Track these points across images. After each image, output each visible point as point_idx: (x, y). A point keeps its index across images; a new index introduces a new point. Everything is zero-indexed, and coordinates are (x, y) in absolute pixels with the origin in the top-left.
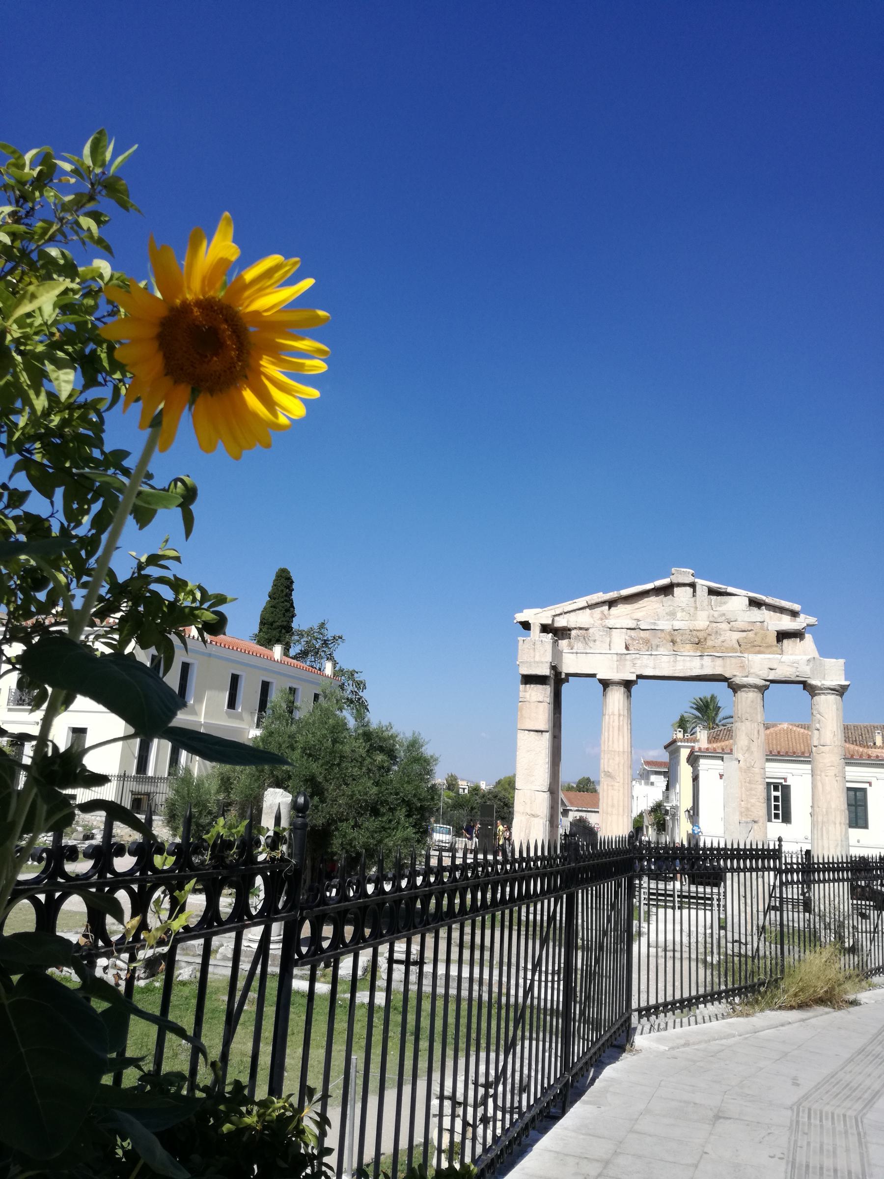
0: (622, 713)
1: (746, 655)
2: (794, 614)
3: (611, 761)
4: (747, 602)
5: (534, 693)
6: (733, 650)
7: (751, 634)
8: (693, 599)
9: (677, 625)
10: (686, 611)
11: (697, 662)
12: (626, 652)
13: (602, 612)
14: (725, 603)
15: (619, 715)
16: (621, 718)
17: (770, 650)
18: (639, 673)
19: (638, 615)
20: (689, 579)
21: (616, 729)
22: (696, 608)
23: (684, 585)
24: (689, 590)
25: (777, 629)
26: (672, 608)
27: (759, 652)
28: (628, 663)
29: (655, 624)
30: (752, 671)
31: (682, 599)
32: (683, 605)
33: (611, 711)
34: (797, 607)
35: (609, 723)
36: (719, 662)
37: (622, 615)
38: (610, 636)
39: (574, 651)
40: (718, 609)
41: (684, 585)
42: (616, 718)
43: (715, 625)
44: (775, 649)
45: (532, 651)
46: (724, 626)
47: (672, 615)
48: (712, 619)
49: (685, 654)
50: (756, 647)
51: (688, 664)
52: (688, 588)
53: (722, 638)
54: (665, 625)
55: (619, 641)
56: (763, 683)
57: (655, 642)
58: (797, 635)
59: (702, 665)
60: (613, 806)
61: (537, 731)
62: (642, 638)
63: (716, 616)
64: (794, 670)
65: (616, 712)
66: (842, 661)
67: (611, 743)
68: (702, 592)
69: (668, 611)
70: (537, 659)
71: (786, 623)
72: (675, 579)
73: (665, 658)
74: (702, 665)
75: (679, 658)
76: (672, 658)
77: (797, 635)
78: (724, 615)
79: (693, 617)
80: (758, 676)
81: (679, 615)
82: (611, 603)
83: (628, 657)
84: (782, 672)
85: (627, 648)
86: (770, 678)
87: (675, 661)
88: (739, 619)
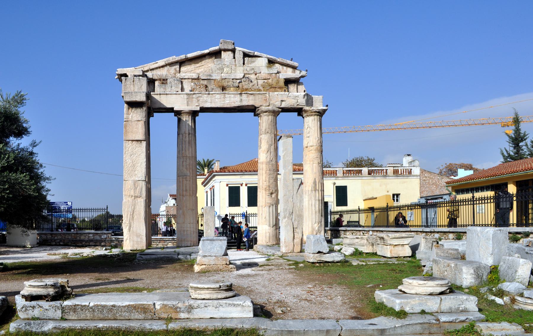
0: (190, 132)
1: (268, 93)
2: (294, 68)
3: (184, 163)
4: (267, 61)
5: (134, 115)
6: (260, 90)
9: (224, 75)
10: (230, 67)
11: (238, 98)
13: (175, 69)
16: (190, 135)
18: (201, 106)
19: (198, 71)
20: (231, 47)
21: (187, 142)
22: (236, 65)
24: (230, 54)
25: (285, 78)
26: (220, 65)
28: (194, 99)
33: (183, 131)
34: (296, 64)
36: (251, 97)
37: (188, 71)
40: (250, 65)
45: (132, 86)
48: (246, 72)
49: (230, 93)
50: (272, 88)
51: (232, 99)
52: (230, 52)
54: (216, 76)
56: (278, 109)
58: (296, 81)
59: (241, 100)
61: (137, 141)
62: (202, 85)
63: (248, 70)
65: (187, 132)
66: (321, 97)
67: (184, 151)
68: (239, 55)
69: (218, 67)
70: (136, 90)
71: (289, 73)
72: (222, 47)
75: (227, 96)
76: (222, 96)
77: (296, 81)
78: (253, 69)
81: (225, 70)
82: (181, 63)
83: (194, 96)
84: (289, 103)
86: (282, 106)
87: (225, 98)
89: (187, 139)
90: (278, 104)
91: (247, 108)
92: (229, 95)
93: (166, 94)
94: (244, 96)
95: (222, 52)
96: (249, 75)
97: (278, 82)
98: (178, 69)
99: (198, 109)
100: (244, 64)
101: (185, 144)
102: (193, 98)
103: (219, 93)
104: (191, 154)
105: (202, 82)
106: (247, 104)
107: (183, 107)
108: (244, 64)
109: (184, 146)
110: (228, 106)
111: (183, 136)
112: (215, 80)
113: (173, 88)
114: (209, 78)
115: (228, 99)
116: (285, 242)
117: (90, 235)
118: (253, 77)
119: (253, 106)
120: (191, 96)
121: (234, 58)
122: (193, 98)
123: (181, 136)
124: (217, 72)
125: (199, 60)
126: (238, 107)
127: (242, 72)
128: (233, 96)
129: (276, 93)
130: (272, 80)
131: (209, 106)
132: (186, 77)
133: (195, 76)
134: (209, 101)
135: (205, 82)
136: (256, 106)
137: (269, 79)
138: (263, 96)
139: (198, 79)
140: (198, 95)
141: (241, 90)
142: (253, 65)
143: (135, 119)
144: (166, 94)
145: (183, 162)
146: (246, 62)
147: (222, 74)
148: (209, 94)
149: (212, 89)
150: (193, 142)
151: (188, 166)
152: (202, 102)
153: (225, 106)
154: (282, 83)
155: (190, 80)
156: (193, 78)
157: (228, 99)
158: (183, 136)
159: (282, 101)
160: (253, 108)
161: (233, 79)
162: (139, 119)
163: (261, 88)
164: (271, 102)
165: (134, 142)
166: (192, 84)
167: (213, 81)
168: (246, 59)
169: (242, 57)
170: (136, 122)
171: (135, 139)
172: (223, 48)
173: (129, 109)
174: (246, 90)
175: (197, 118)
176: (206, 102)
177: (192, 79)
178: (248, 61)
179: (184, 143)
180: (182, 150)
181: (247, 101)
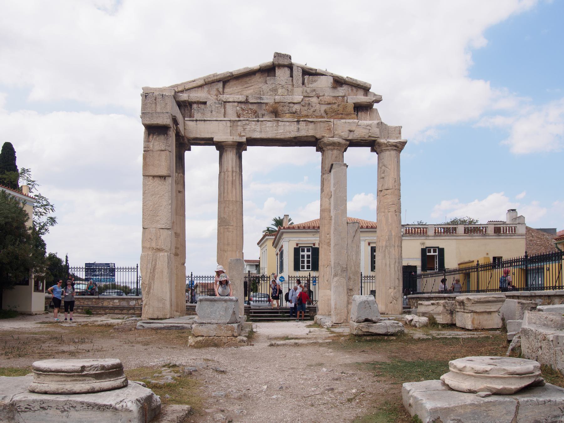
0: (234, 169)
1: (332, 120)
3: (226, 209)
5: (156, 143)
6: (322, 117)
7: (335, 106)
8: (291, 78)
9: (278, 98)
11: (294, 127)
12: (237, 119)
13: (218, 90)
14: (315, 81)
15: (233, 172)
16: (234, 174)
17: (350, 117)
18: (248, 136)
22: (293, 85)
23: (284, 66)
24: (287, 71)
25: (354, 101)
26: (274, 86)
27: (342, 118)
28: (239, 128)
29: (260, 98)
30: (336, 132)
31: (282, 78)
32: (283, 83)
35: (224, 178)
36: (311, 126)
38: (225, 108)
39: (194, 119)
40: (310, 85)
41: (284, 66)
42: (230, 174)
43: (307, 99)
44: (353, 116)
45: (154, 106)
46: (314, 100)
47: (275, 90)
48: (305, 94)
49: (285, 120)
50: (340, 114)
51: (288, 128)
53: (312, 109)
54: (268, 99)
55: (232, 112)
56: (343, 142)
57: (260, 113)
59: (299, 129)
60: (228, 244)
62: (251, 109)
63: (308, 91)
64: (368, 131)
65: (230, 169)
67: (226, 194)
69: (271, 87)
73: (269, 124)
74: (299, 129)
75: (280, 123)
76: (275, 124)
78: (314, 90)
79: (290, 92)
80: (340, 137)
81: (280, 91)
83: (239, 123)
84: (360, 133)
85: (239, 117)
86: (350, 138)
88: (326, 94)
89: (230, 179)
90: (345, 134)
91: (305, 139)
92: (283, 123)
93: (204, 121)
94: (302, 124)
95: (276, 69)
96: (310, 99)
97: (345, 107)
98: (221, 90)
99: (244, 140)
100: (303, 84)
101: (227, 185)
102: (238, 126)
103: (271, 119)
104: (234, 197)
105: (250, 106)
106: (306, 134)
107: (225, 137)
108: (303, 84)
109: (226, 186)
110: (282, 137)
111: (224, 175)
112: (266, 104)
113: (214, 113)
114: (259, 101)
115: (282, 127)
116: (335, 308)
117: (115, 301)
118: (314, 100)
119: (313, 137)
120: (235, 124)
121: (292, 76)
122: (238, 126)
123: (222, 174)
124: (269, 94)
125: (247, 79)
126: (295, 138)
127: (301, 94)
128: (288, 124)
129: (343, 121)
130: (339, 106)
131: (258, 137)
132: (231, 100)
133: (242, 98)
134: (258, 129)
135: (254, 107)
136: (318, 136)
137: (335, 103)
138: (326, 125)
139: (246, 102)
140: (244, 122)
141: (298, 118)
142: (314, 85)
143: (157, 148)
144: (204, 121)
145: (224, 208)
146: (306, 81)
147: (276, 97)
148: (258, 121)
149: (263, 115)
150: (238, 182)
151: (231, 213)
152: (250, 131)
153: (278, 137)
154: (351, 108)
155: (236, 104)
156: (239, 100)
157: (282, 127)
158: (224, 175)
159: (350, 131)
160: (314, 140)
161: (289, 103)
162: (163, 149)
163: (324, 115)
164: (336, 132)
165: (156, 179)
166: (238, 108)
167: (264, 106)
168: (306, 77)
169: (301, 74)
170: (159, 152)
171: (157, 174)
172: (276, 63)
173: (149, 135)
174: (307, 116)
175: (244, 153)
176: (254, 131)
177: (238, 102)
178: (308, 80)
179: (226, 183)
180: (224, 193)
181: (306, 131)
